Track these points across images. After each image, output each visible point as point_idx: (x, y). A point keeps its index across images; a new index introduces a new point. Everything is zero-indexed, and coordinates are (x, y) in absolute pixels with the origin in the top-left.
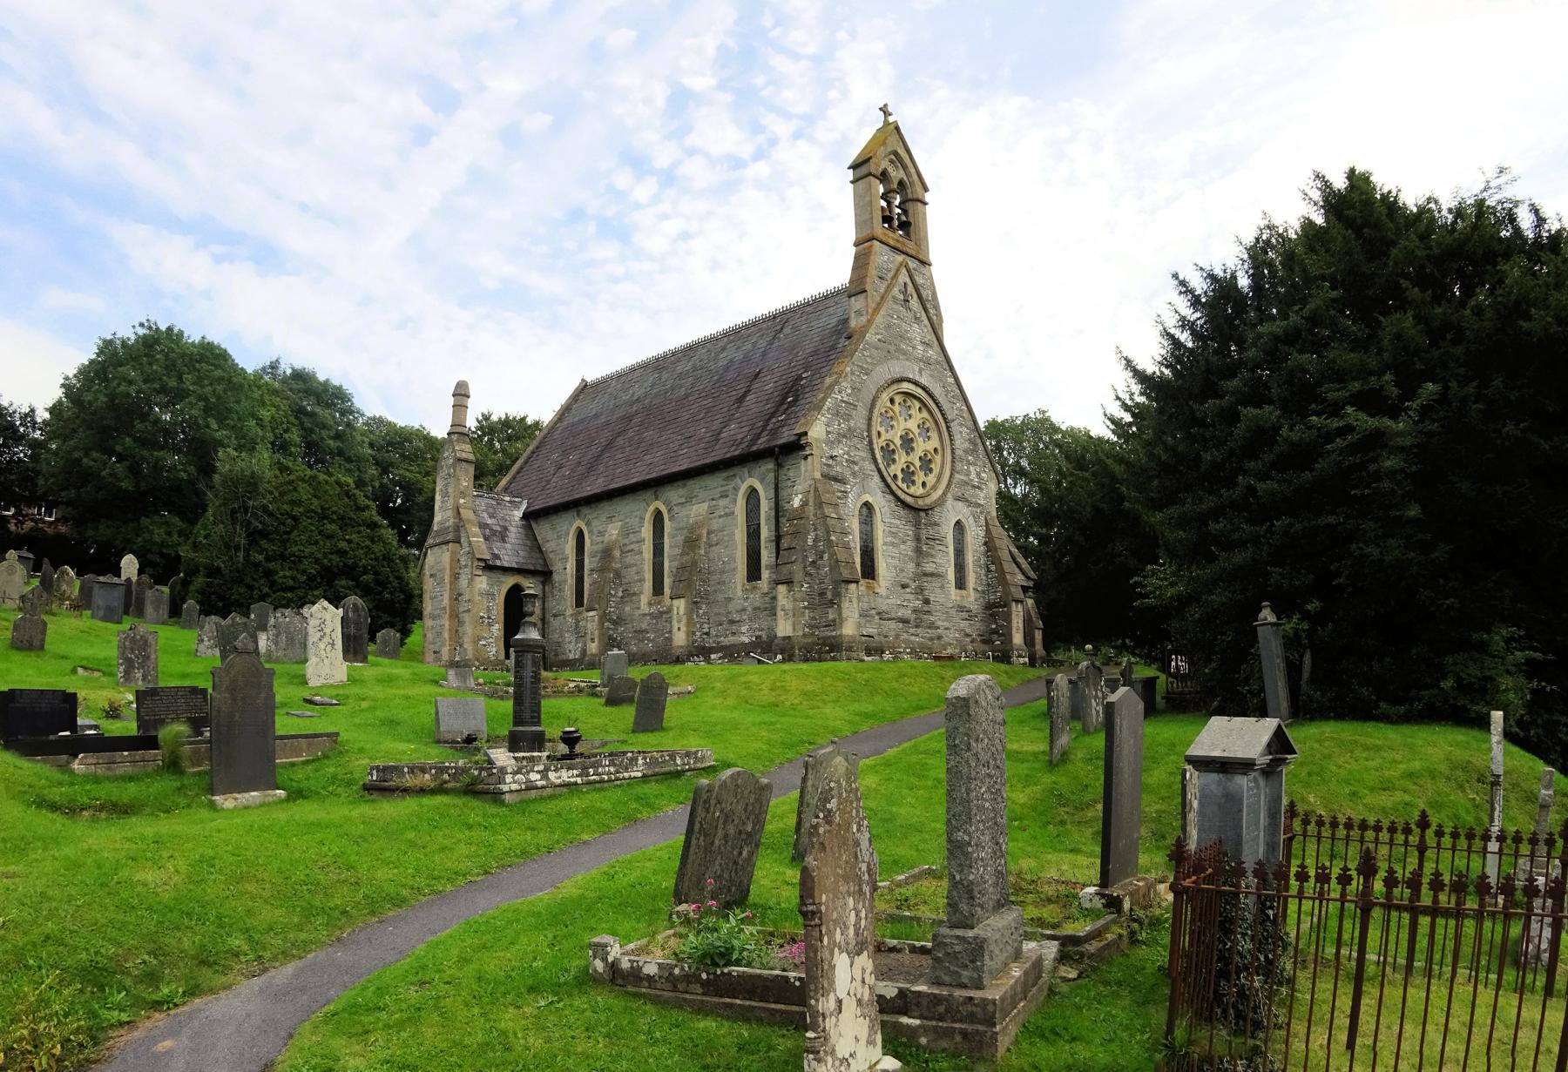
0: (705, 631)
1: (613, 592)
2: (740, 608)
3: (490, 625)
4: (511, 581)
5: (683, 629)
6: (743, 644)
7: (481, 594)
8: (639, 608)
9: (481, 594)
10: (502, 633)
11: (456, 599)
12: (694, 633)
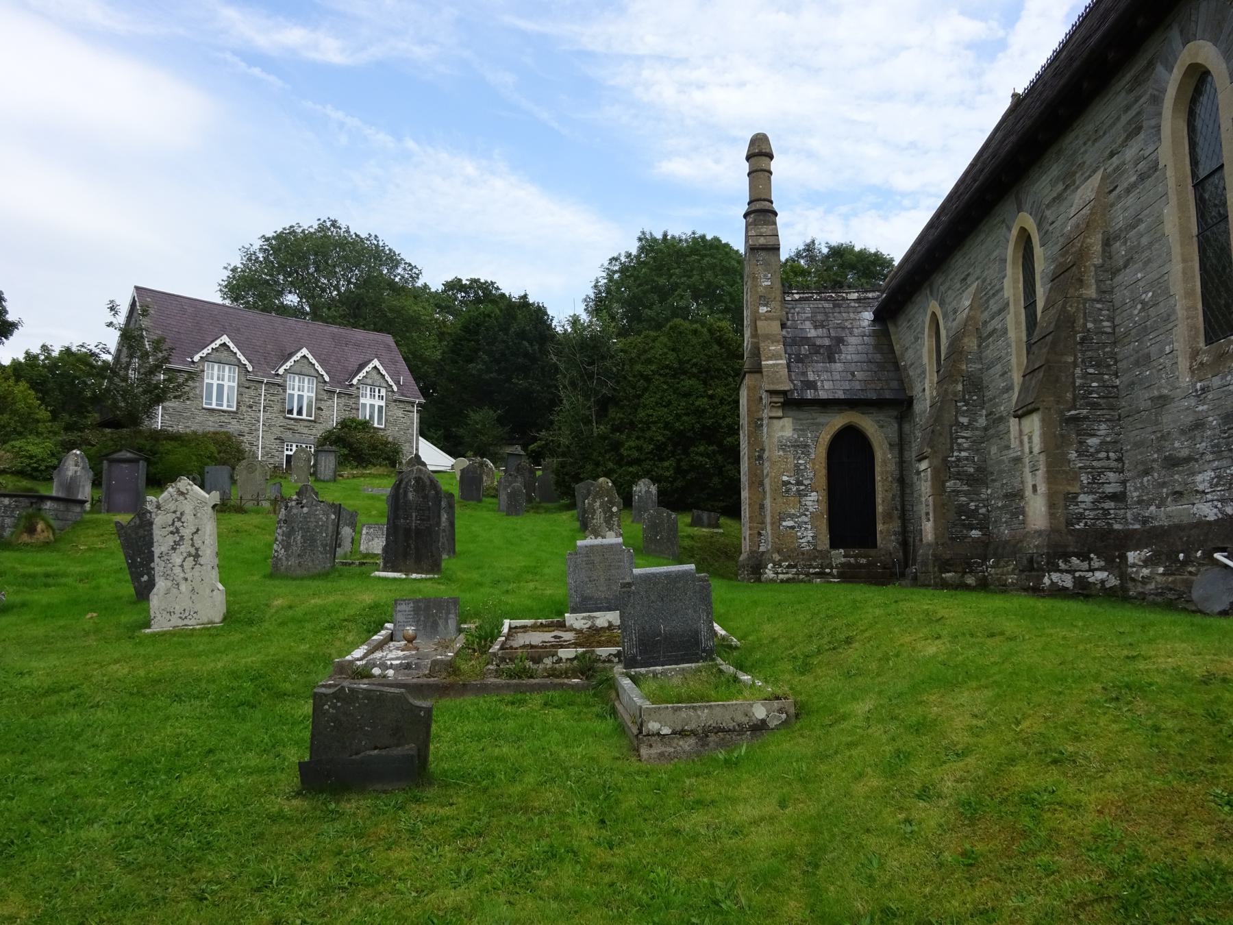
0: (1109, 489)
1: (964, 420)
2: (1188, 420)
3: (801, 494)
4: (837, 421)
5: (1042, 488)
6: (1202, 524)
7: (783, 447)
8: (1008, 447)
9: (783, 447)
10: (824, 507)
11: (760, 458)
12: (1072, 498)
